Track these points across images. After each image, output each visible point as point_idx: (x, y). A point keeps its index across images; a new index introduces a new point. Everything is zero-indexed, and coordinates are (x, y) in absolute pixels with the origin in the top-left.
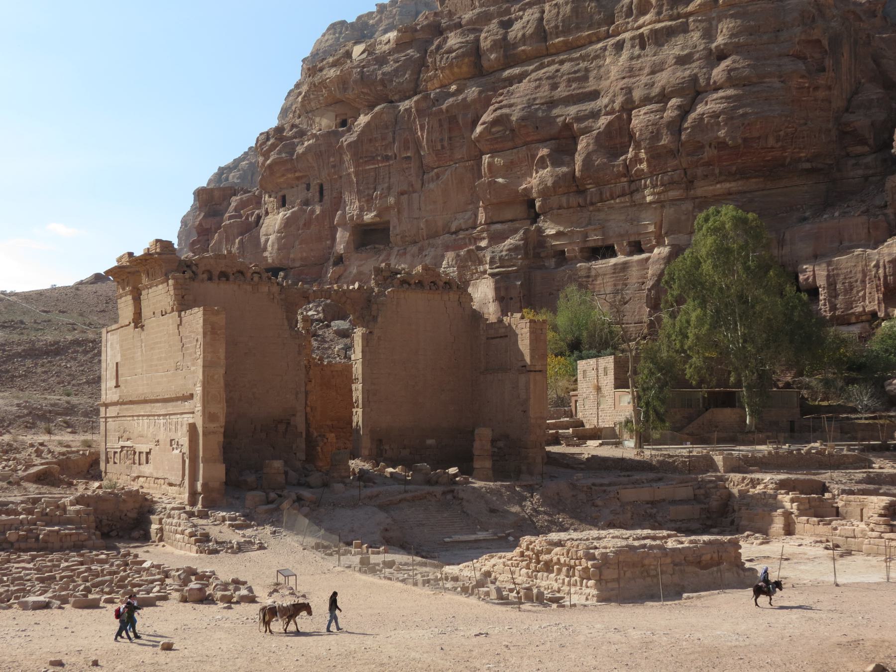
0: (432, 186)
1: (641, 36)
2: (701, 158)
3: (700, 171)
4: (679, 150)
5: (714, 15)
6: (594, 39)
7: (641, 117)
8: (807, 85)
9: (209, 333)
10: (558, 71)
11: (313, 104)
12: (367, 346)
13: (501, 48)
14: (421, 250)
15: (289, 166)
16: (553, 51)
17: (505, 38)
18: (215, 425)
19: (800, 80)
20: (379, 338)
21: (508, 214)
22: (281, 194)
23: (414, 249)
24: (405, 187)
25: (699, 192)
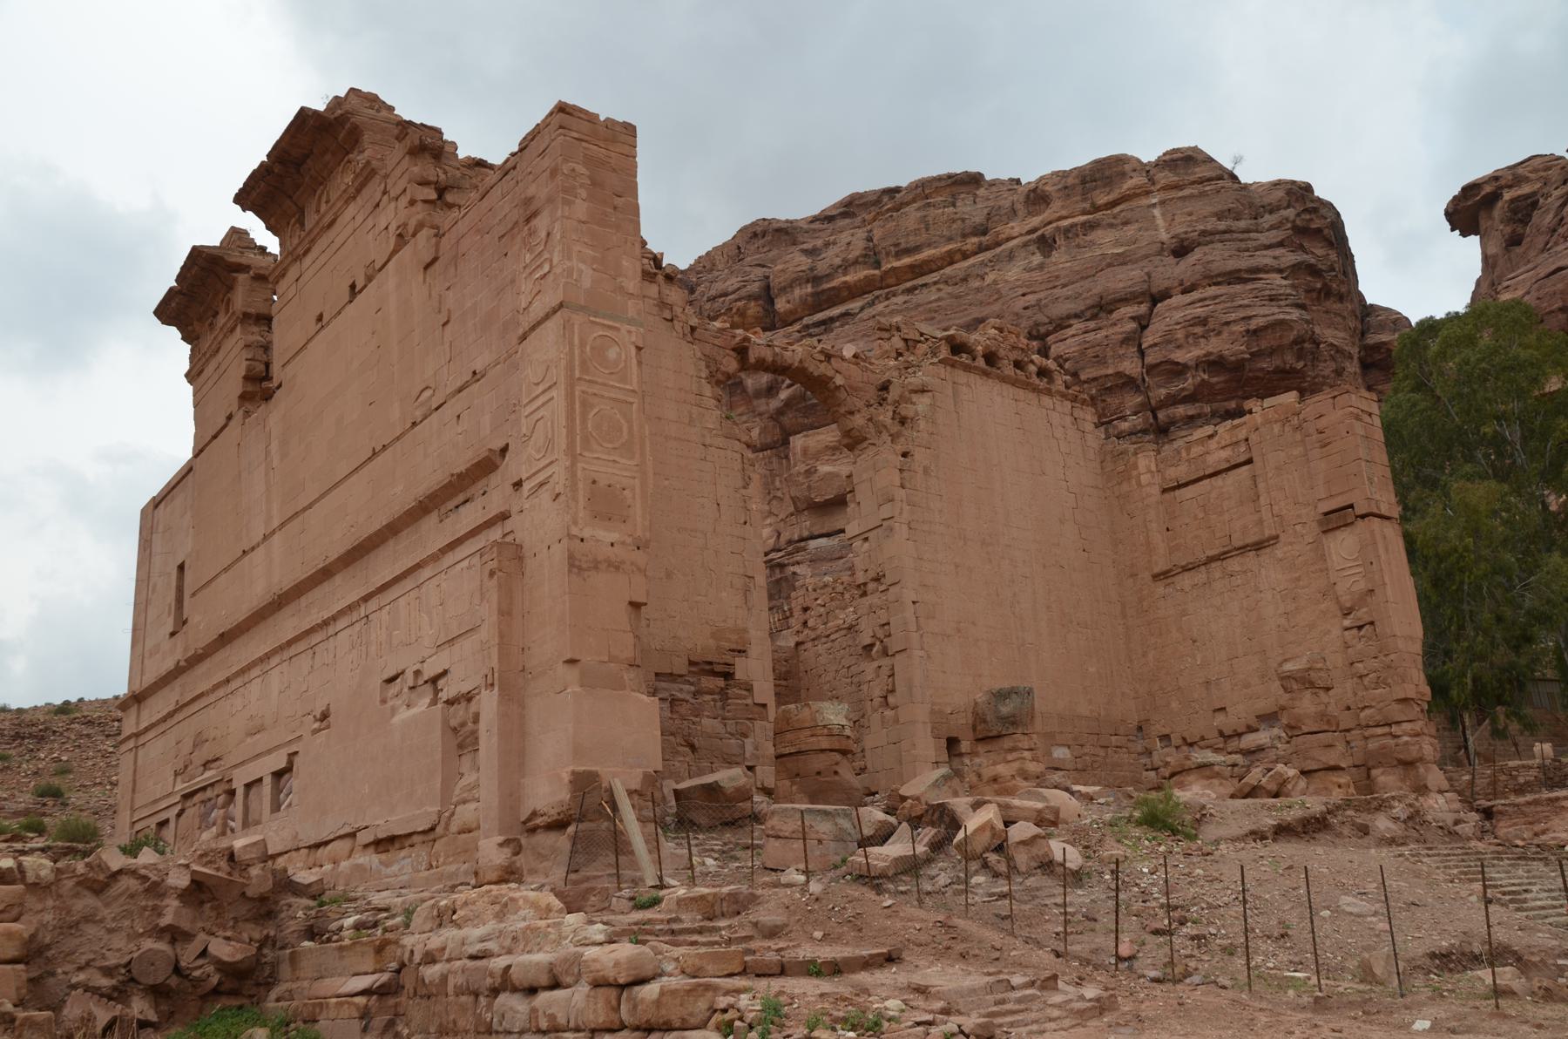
1: (1042, 239)
2: (1183, 389)
3: (1181, 410)
4: (1144, 380)
5: (1154, 201)
6: (958, 256)
7: (1068, 341)
8: (1319, 285)
9: (583, 193)
10: (905, 302)
12: (903, 487)
13: (808, 281)
16: (891, 281)
17: (812, 269)
18: (614, 536)
19: (1309, 278)
20: (926, 471)
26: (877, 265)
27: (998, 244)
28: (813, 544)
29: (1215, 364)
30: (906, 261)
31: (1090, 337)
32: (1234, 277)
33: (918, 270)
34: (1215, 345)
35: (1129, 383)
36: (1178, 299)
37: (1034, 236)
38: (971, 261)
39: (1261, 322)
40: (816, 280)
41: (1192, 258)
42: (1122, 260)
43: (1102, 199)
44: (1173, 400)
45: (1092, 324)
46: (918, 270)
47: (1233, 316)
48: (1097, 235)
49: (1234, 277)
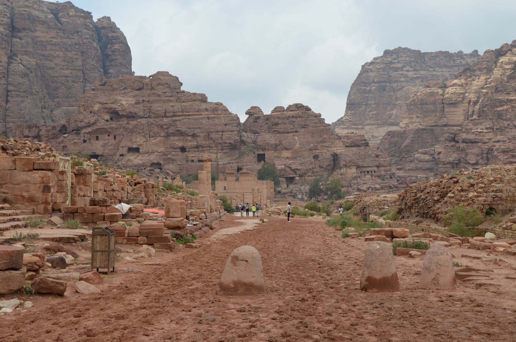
0: (154, 141)
3: (225, 148)
11: (101, 112)
14: (149, 155)
15: (105, 130)
21: (177, 150)
22: (97, 135)
23: (147, 155)
24: (145, 140)
25: (224, 151)
26: (183, 113)
27: (201, 115)
28: (173, 153)
29: (230, 143)
30: (187, 114)
31: (216, 136)
32: (232, 131)
33: (189, 115)
34: (230, 141)
35: (221, 144)
36: (226, 133)
37: (207, 116)
38: (197, 117)
39: (235, 139)
40: (174, 112)
41: (228, 126)
42: (219, 125)
43: (216, 113)
44: (225, 146)
45: (216, 134)
46: (189, 115)
47: (233, 138)
48: (215, 119)
49: (232, 131)
